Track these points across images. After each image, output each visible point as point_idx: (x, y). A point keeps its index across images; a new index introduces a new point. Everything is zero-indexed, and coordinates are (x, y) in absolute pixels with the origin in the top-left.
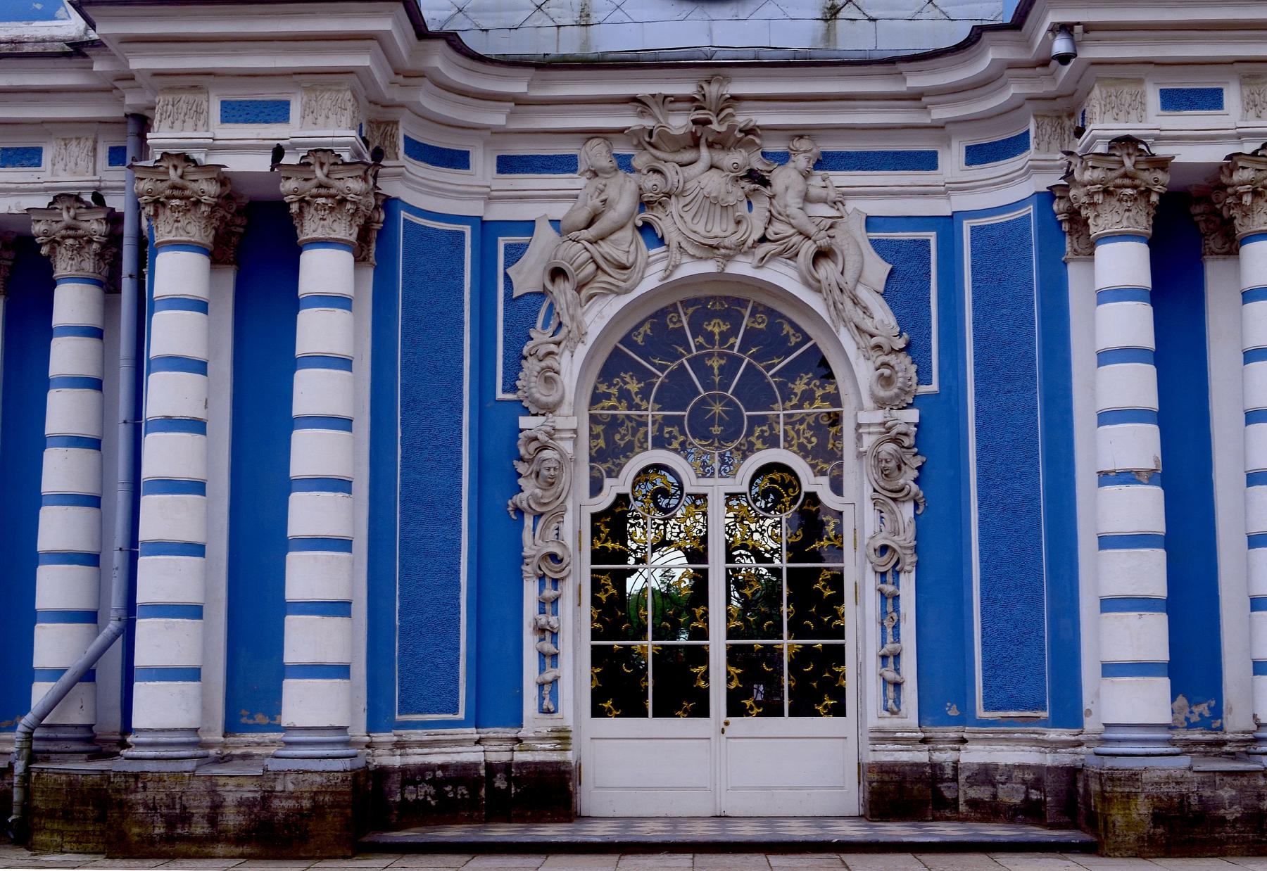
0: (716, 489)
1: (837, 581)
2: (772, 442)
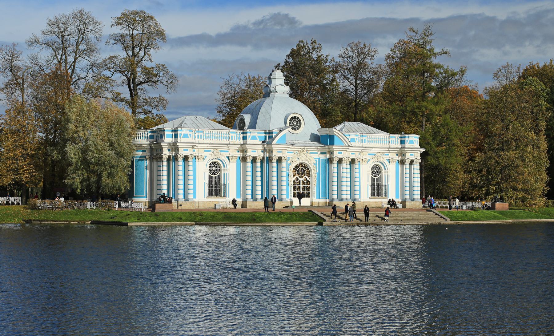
0: (301, 179)
1: (309, 187)
2: (305, 175)
